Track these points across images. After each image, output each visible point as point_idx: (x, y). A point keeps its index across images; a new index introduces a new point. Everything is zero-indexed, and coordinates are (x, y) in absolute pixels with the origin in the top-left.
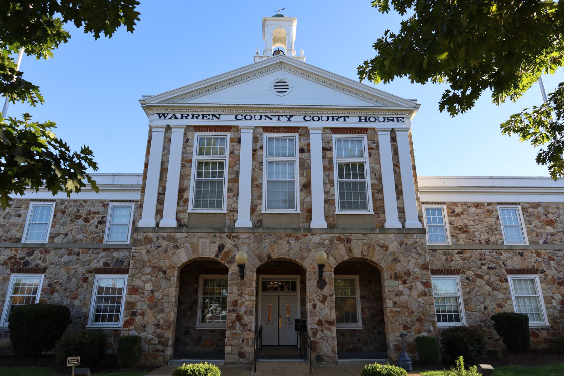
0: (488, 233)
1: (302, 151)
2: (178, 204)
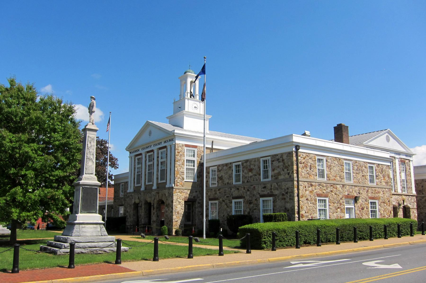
0: (228, 179)
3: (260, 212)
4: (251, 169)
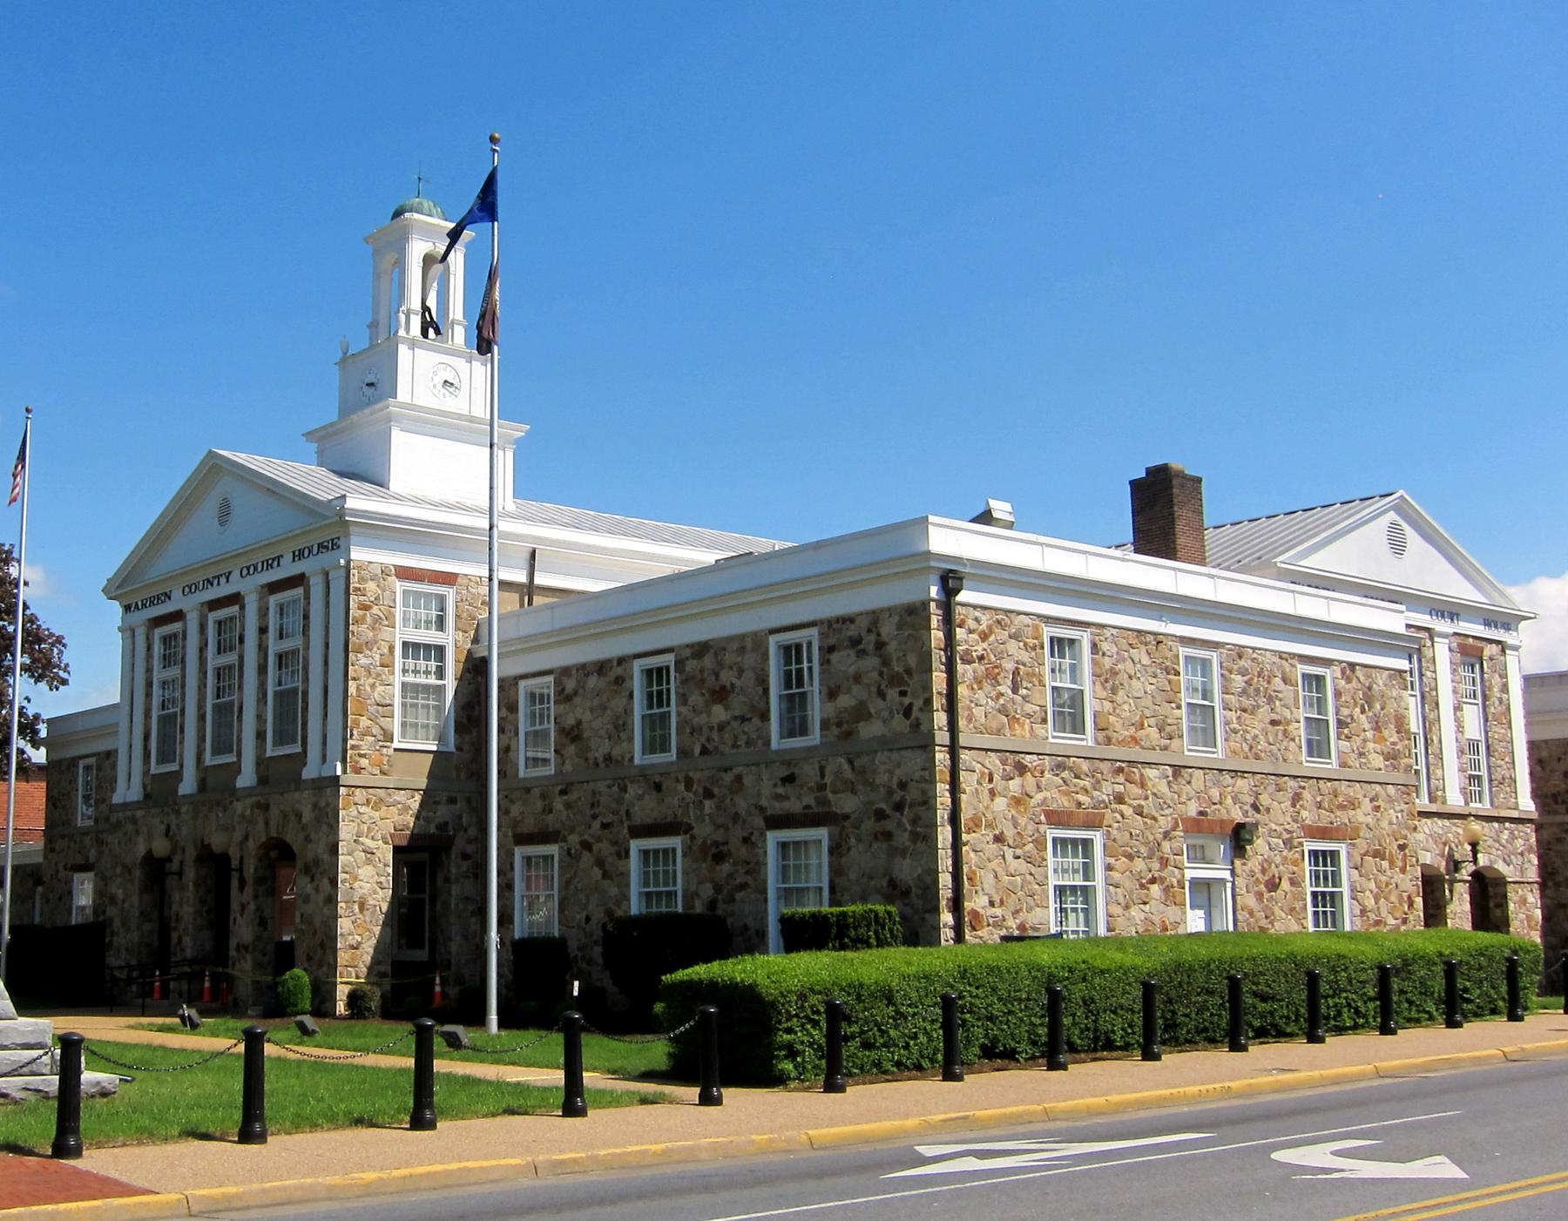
0: (610, 738)
3: (766, 900)
4: (723, 688)
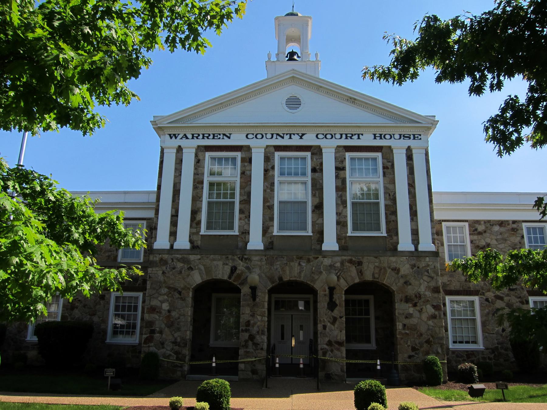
1: (314, 170)
2: (191, 226)
